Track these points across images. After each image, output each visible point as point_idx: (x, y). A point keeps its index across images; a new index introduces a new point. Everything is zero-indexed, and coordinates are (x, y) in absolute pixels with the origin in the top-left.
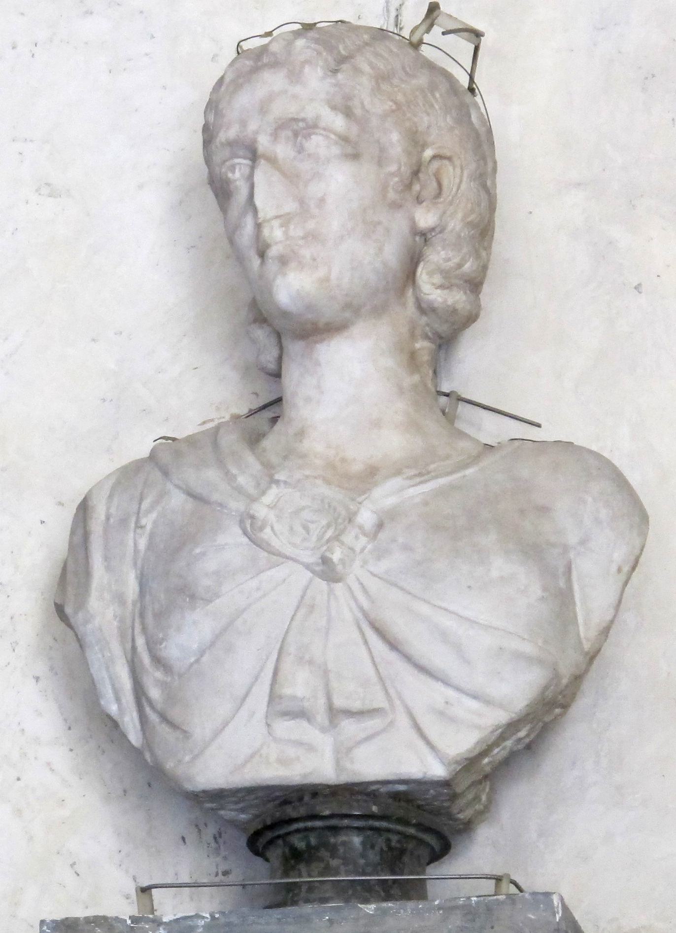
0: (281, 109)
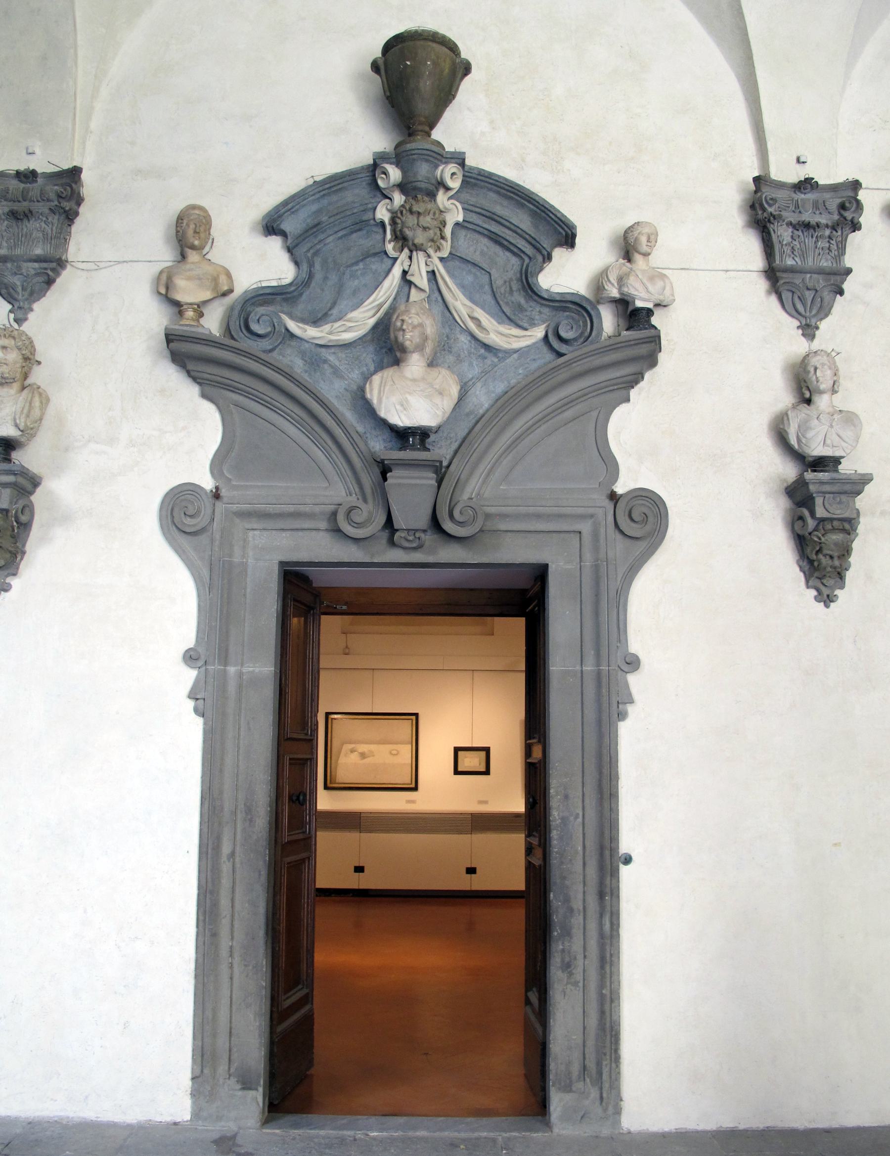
0: (821, 362)
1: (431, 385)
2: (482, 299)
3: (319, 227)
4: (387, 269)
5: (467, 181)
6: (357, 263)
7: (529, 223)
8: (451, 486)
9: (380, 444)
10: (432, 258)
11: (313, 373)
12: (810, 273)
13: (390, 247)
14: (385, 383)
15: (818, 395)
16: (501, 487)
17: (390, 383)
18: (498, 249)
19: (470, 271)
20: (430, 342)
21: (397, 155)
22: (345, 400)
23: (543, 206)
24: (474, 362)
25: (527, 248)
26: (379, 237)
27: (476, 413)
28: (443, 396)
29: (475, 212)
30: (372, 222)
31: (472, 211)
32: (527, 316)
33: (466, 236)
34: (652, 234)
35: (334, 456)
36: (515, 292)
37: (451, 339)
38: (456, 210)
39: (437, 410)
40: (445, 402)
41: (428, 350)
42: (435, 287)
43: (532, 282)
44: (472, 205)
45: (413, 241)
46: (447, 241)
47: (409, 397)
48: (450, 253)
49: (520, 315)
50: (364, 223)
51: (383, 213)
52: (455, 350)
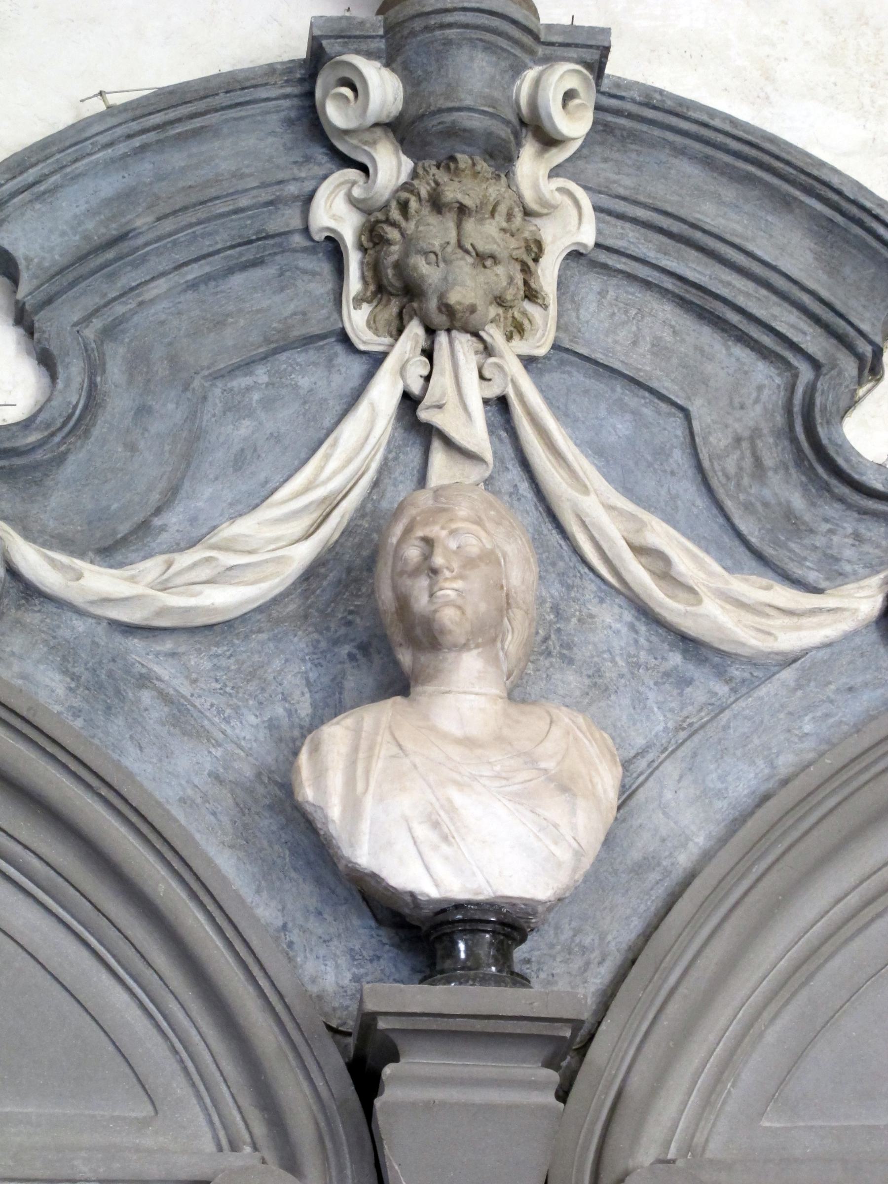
1: (531, 760)
2: (663, 492)
3: (125, 246)
4: (347, 389)
5: (606, 125)
6: (247, 365)
7: (809, 256)
8: (594, 1123)
9: (337, 966)
10: (501, 357)
11: (100, 718)
14: (371, 748)
16: (765, 1123)
17: (386, 749)
19: (622, 406)
20: (518, 615)
21: (391, 30)
22: (214, 814)
23: (854, 202)
25: (805, 333)
26: (322, 287)
27: (665, 863)
28: (574, 795)
29: (635, 221)
30: (298, 240)
31: (621, 217)
32: (815, 548)
33: (602, 294)
35: (173, 1007)
36: (770, 474)
37: (568, 620)
38: (574, 212)
39: (556, 843)
40: (581, 819)
42: (508, 452)
43: (829, 439)
44: (624, 199)
45: (442, 297)
46: (545, 307)
47: (457, 797)
48: (556, 347)
49: (792, 545)
50: (271, 242)
52: (581, 654)
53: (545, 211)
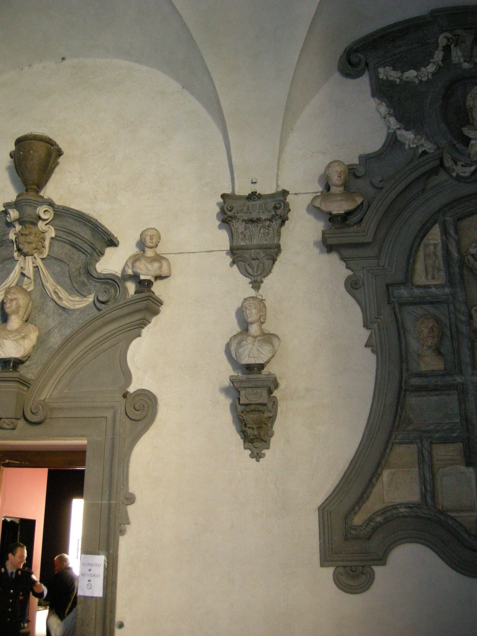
12: (253, 249)
13: (16, 254)
15: (250, 325)
18: (75, 250)
24: (56, 318)
25: (88, 249)
27: (54, 347)
34: (153, 235)
41: (21, 313)
46: (46, 249)
51: (12, 236)
53: (45, 232)
